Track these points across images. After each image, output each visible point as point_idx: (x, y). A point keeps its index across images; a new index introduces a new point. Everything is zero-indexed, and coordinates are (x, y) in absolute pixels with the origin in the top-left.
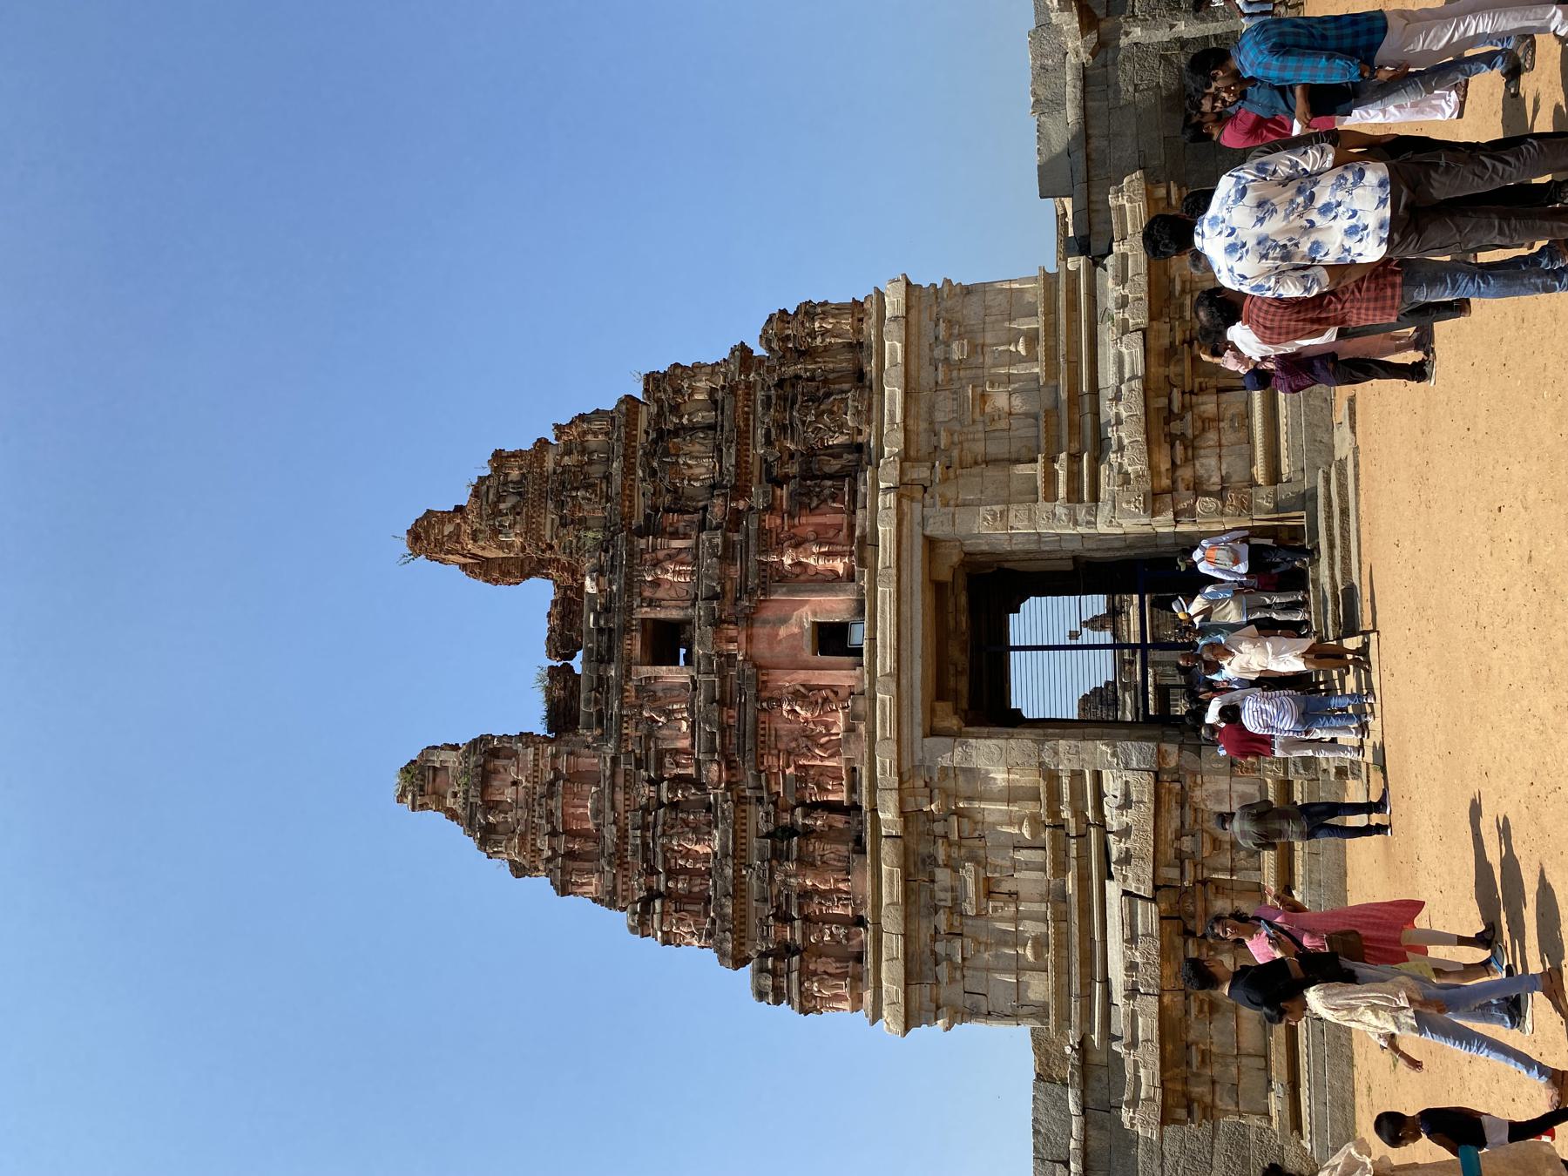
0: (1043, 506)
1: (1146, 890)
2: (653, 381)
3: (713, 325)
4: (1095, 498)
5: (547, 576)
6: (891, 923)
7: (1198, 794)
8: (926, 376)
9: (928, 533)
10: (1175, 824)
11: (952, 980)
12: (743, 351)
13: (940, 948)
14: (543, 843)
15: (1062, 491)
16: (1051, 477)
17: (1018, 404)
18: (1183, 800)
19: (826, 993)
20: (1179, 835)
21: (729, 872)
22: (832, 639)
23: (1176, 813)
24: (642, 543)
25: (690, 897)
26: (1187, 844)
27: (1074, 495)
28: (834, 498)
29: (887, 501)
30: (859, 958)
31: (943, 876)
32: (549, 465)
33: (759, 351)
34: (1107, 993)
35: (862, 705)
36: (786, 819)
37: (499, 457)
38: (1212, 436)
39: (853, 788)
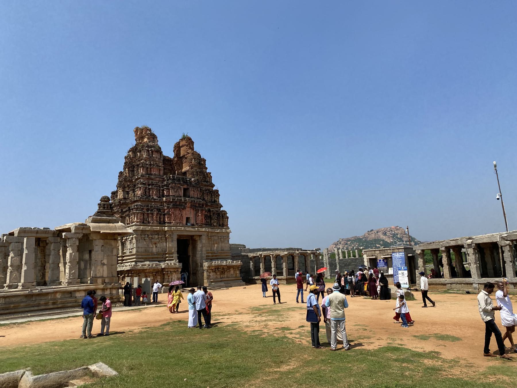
0: (205, 252)
2: (217, 191)
3: (226, 202)
5: (174, 157)
8: (219, 235)
12: (221, 206)
16: (208, 253)
17: (215, 248)
18: (175, 272)
19: (139, 217)
25: (145, 192)
26: (169, 272)
31: (156, 236)
32: (204, 170)
33: (222, 209)
39: (168, 223)
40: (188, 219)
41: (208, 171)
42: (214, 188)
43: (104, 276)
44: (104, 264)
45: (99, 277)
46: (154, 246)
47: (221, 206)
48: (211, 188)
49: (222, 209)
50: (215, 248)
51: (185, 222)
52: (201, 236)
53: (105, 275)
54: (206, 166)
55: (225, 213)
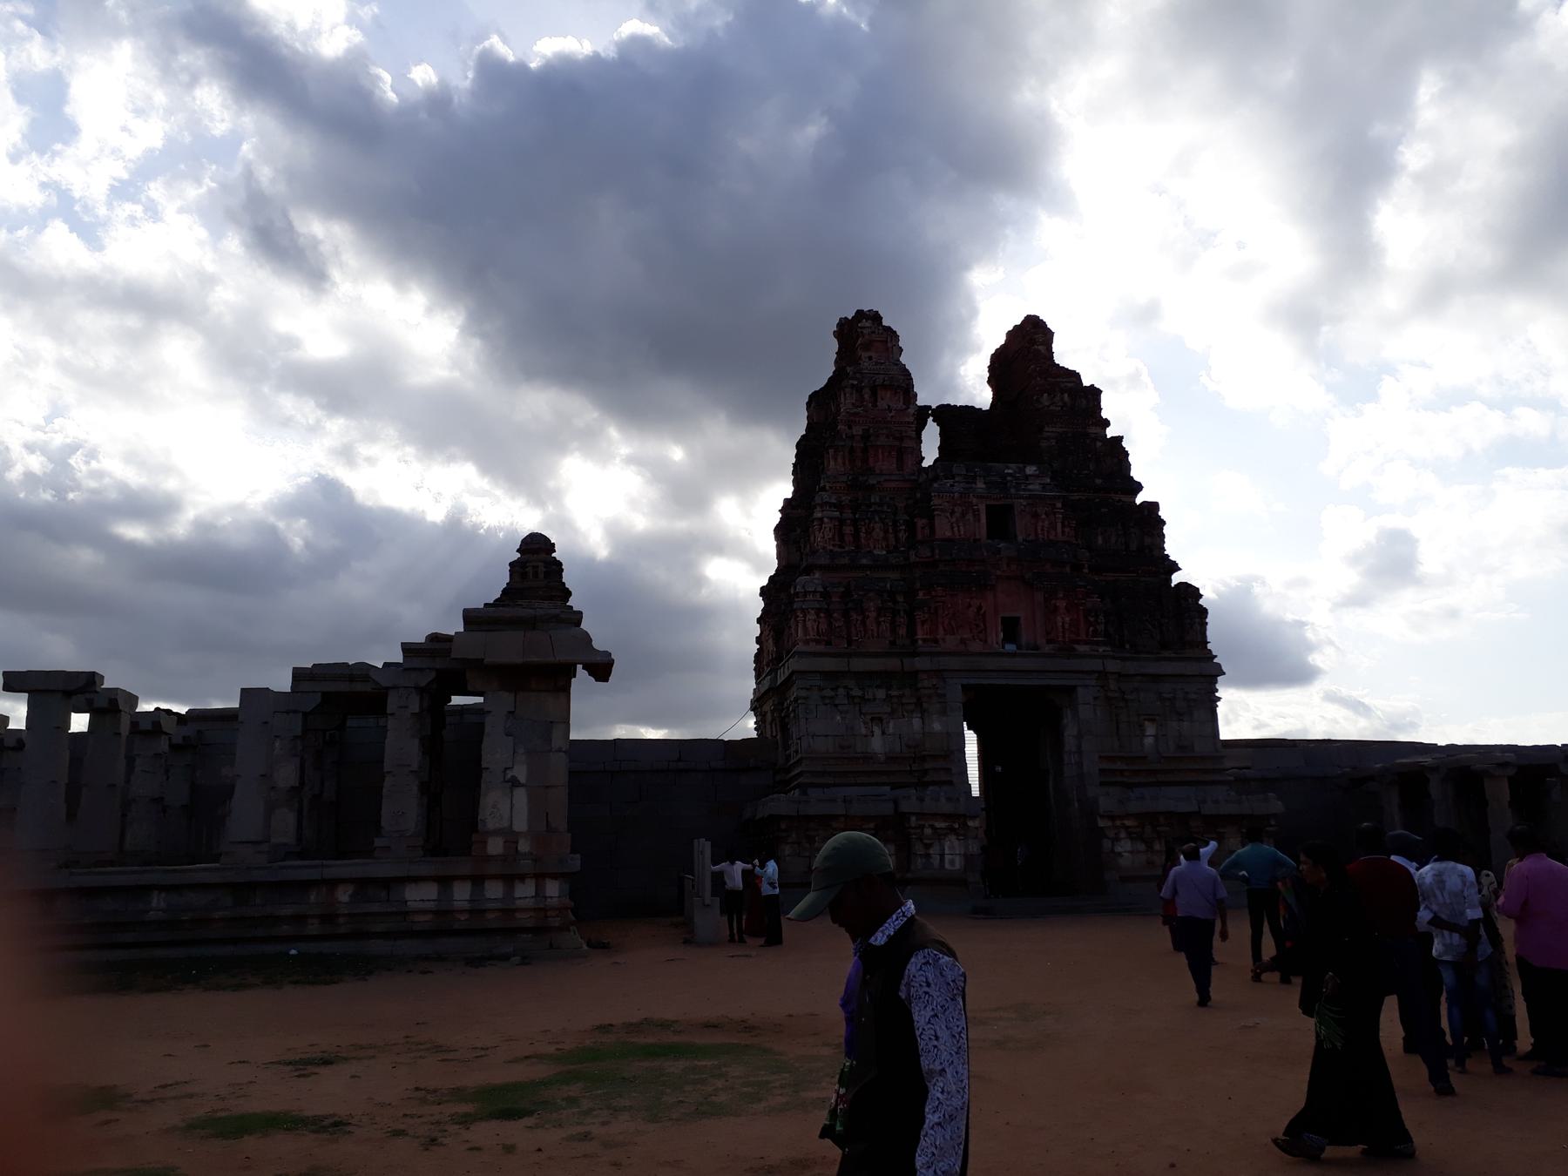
1: (905, 807)
2: (1154, 506)
4: (1102, 784)
6: (859, 664)
7: (953, 838)
9: (1080, 690)
10: (937, 825)
11: (823, 698)
12: (1175, 567)
13: (841, 691)
14: (857, 430)
15: (1105, 766)
17: (1149, 741)
18: (952, 830)
19: (809, 624)
20: (932, 827)
21: (864, 561)
22: (1011, 629)
23: (943, 825)
24: (1059, 505)
25: (842, 536)
26: (928, 831)
27: (1102, 771)
28: (1095, 631)
29: (1096, 665)
30: (828, 643)
31: (881, 694)
33: (1176, 578)
34: (828, 786)
35: (976, 646)
36: (900, 599)
37: (1095, 393)
38: (1142, 847)
39: (924, 640)
40: (1011, 629)
41: (1110, 432)
42: (1139, 500)
43: (516, 828)
44: (514, 783)
45: (497, 832)
46: (877, 731)
47: (1175, 567)
48: (1125, 499)
49: (1176, 578)
50: (1149, 741)
51: (996, 635)
52: (1074, 688)
53: (520, 824)
54: (1104, 415)
55: (1190, 593)
